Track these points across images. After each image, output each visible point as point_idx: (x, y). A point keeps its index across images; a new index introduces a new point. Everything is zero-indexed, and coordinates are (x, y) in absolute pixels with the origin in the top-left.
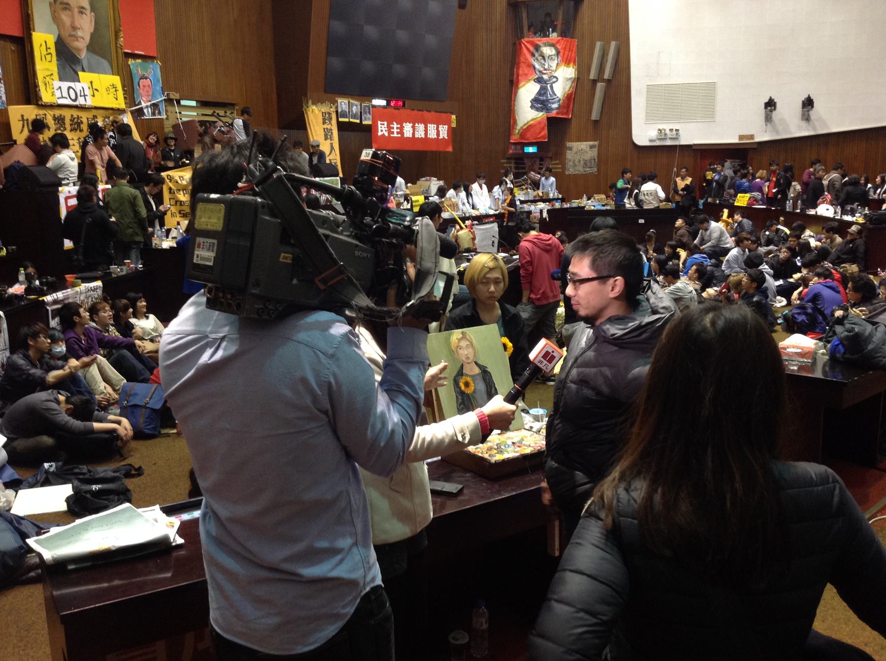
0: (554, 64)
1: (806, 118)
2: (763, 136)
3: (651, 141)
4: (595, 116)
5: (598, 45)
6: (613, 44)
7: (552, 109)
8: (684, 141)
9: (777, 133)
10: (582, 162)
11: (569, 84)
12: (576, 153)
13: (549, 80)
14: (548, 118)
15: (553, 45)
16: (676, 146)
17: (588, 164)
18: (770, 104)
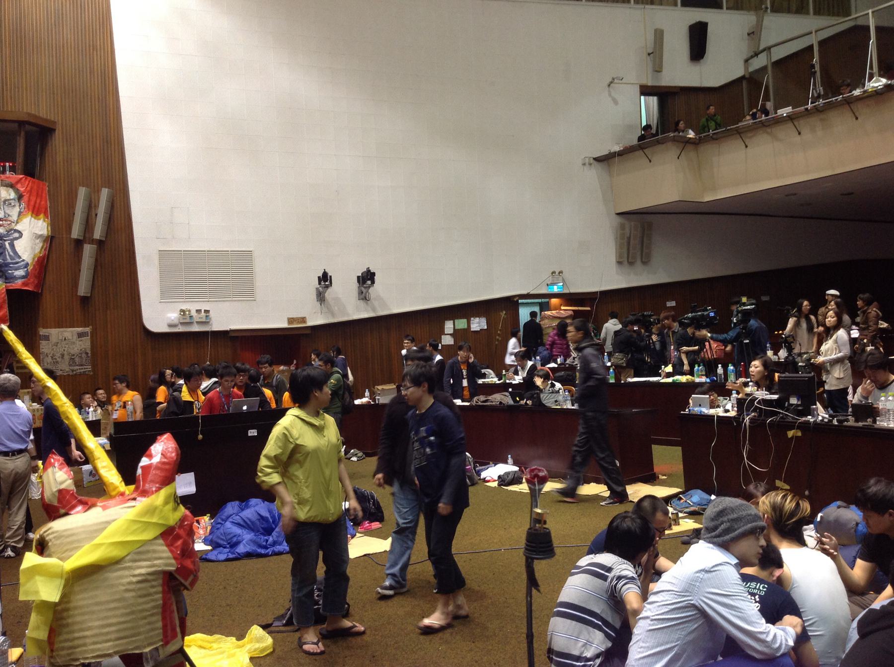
0: (14, 213)
1: (364, 297)
2: (316, 319)
3: (170, 326)
4: (83, 289)
5: (82, 192)
6: (105, 193)
7: (15, 278)
8: (217, 325)
9: (333, 315)
10: (66, 357)
11: (39, 245)
12: (56, 344)
13: (8, 235)
14: (9, 292)
15: (12, 186)
16: (207, 332)
17: (77, 360)
18: (325, 278)
